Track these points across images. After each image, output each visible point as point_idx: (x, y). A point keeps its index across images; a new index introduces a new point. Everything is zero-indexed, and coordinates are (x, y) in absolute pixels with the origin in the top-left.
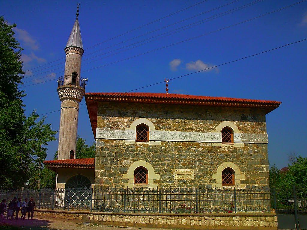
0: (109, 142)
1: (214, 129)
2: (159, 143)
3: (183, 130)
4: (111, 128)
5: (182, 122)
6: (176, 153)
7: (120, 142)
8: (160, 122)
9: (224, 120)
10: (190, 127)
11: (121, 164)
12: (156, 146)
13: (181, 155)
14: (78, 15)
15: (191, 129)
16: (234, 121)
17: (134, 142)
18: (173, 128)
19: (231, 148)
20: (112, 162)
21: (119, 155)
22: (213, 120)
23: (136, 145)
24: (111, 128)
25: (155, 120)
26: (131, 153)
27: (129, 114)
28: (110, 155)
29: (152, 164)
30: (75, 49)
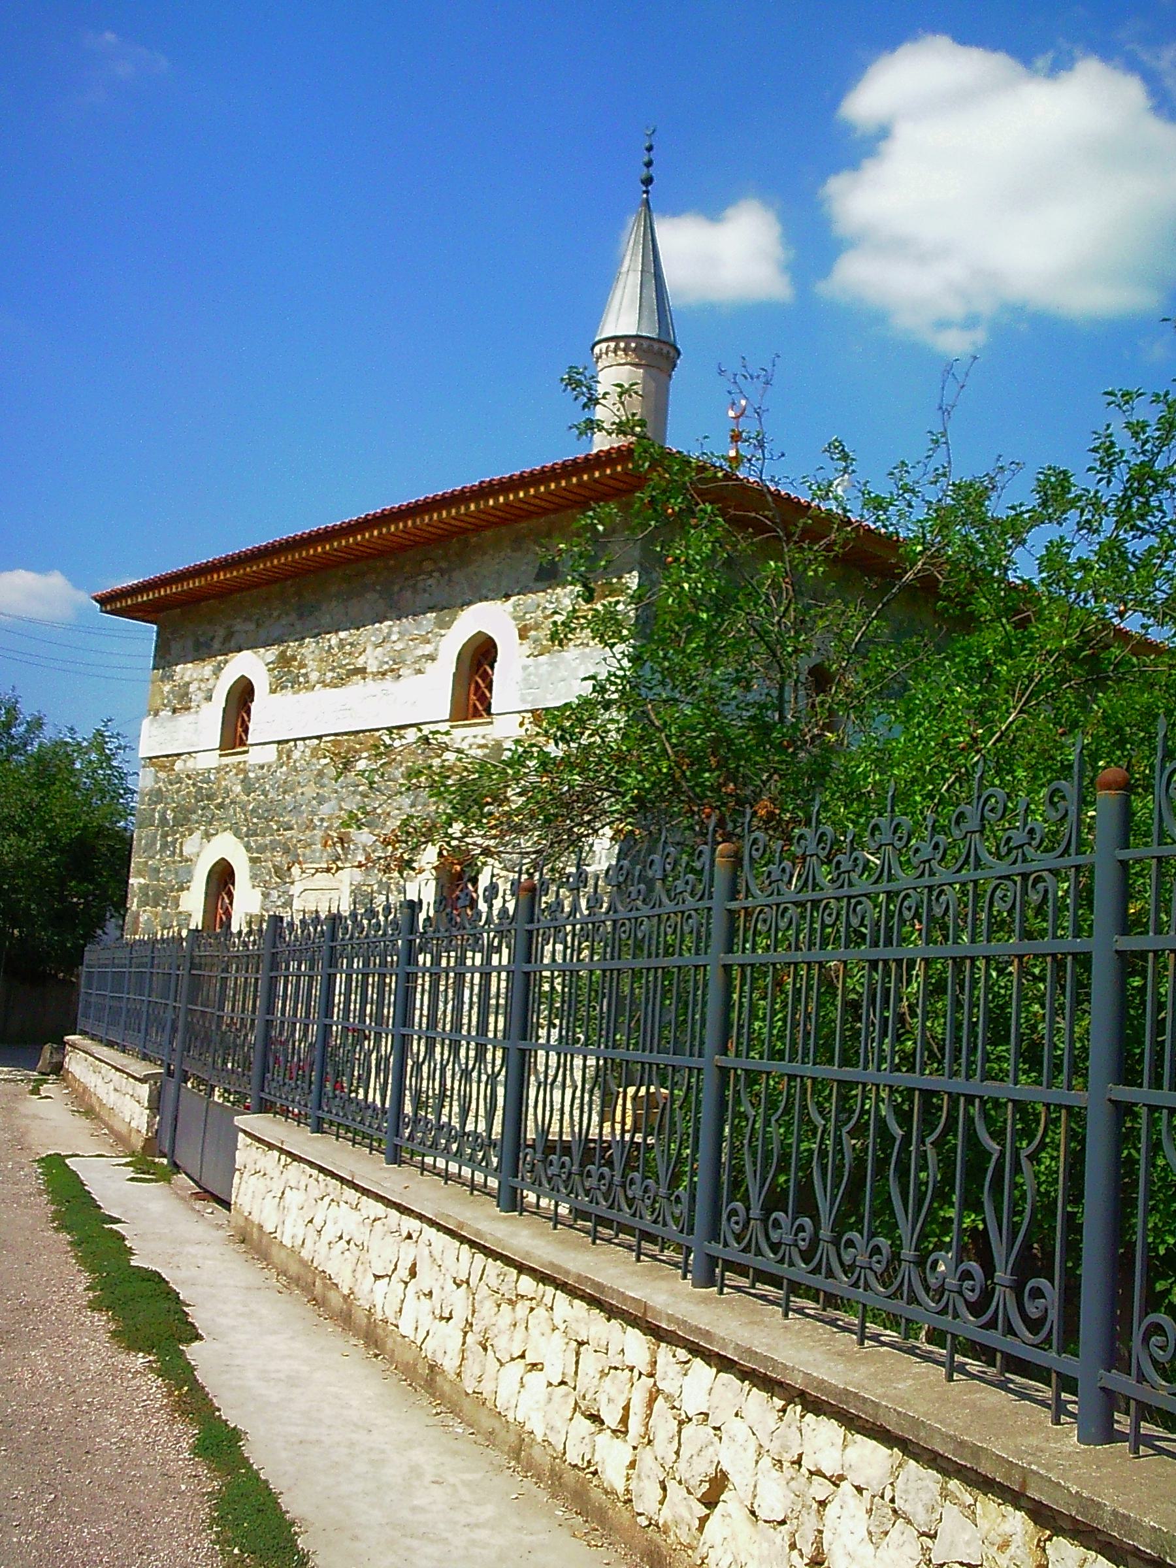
0: (163, 767)
1: (432, 658)
2: (269, 754)
3: (340, 682)
4: (174, 711)
5: (341, 645)
6: (311, 791)
7: (191, 764)
8: (284, 661)
9: (469, 603)
10: (360, 663)
11: (181, 855)
12: (262, 767)
13: (321, 800)
14: (648, 181)
15: (362, 671)
16: (507, 596)
17: (210, 760)
18: (314, 676)
19: (480, 746)
20: (165, 846)
21: (183, 818)
22: (431, 609)
23: (218, 770)
24: (174, 711)
25: (272, 653)
26: (200, 805)
27: (216, 645)
28: (163, 820)
29: (248, 848)
30: (612, 345)
